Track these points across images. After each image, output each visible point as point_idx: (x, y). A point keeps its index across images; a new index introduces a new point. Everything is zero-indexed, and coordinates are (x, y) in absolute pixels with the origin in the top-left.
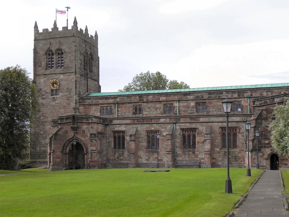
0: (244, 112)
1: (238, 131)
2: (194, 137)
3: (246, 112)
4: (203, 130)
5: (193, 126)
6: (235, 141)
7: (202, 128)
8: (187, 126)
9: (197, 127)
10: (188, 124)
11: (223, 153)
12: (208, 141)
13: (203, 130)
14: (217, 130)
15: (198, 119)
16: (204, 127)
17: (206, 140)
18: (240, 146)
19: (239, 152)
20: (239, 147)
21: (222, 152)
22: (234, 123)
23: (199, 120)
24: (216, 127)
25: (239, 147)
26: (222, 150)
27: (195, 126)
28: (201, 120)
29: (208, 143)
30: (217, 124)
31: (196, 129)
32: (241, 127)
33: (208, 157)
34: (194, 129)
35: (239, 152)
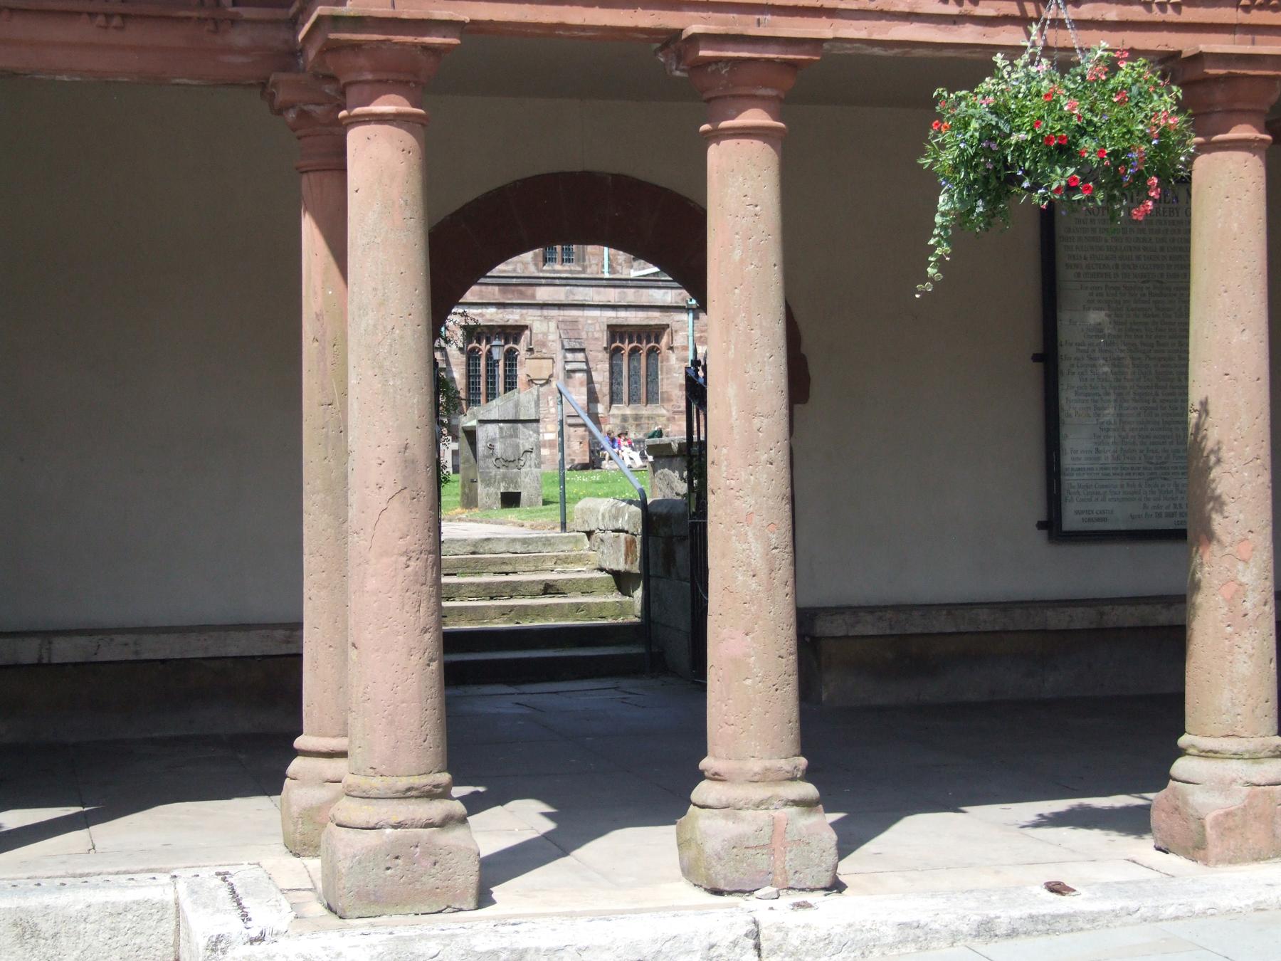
0: (589, 270)
1: (665, 340)
2: (511, 357)
3: (594, 268)
4: (545, 334)
5: (512, 317)
6: (652, 377)
7: (542, 326)
8: (488, 317)
9: (527, 323)
10: (492, 310)
11: (618, 421)
12: (578, 375)
13: (545, 334)
14: (596, 335)
15: (529, 290)
16: (553, 325)
17: (574, 371)
18: (674, 397)
19: (668, 419)
20: (669, 400)
21: (612, 420)
22: (656, 314)
23: (533, 296)
24: (595, 325)
25: (669, 400)
26: (614, 411)
27: (517, 317)
28: (543, 294)
29: (581, 384)
30: (596, 313)
31: (525, 327)
32: (675, 326)
33: (583, 438)
34: (513, 333)
35: (668, 419)
